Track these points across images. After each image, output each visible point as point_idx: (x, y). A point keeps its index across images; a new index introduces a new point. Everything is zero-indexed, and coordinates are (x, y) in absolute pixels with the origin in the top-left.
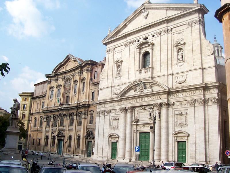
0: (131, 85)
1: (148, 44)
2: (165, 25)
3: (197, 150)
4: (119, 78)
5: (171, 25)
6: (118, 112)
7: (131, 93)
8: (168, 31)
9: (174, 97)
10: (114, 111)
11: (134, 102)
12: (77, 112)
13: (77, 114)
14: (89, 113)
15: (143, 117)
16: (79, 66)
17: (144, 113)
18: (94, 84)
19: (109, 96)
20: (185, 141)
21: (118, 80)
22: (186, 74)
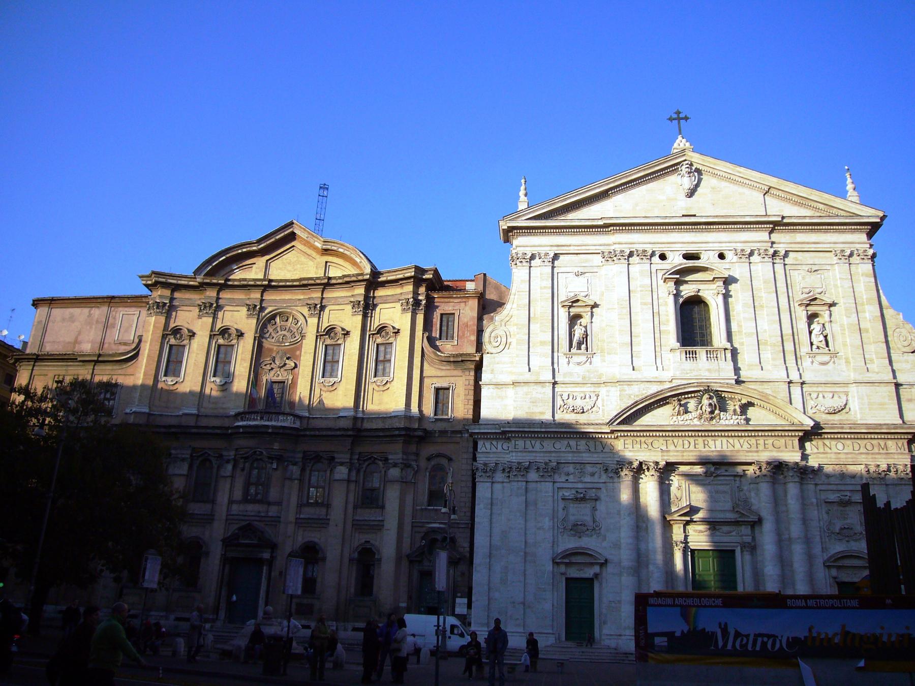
0: (667, 392)
6: (593, 475)
8: (775, 253)
10: (571, 469)
11: (672, 447)
12: (352, 454)
13: (351, 459)
14: (423, 463)
18: (452, 359)
21: (579, 364)
22: (845, 389)
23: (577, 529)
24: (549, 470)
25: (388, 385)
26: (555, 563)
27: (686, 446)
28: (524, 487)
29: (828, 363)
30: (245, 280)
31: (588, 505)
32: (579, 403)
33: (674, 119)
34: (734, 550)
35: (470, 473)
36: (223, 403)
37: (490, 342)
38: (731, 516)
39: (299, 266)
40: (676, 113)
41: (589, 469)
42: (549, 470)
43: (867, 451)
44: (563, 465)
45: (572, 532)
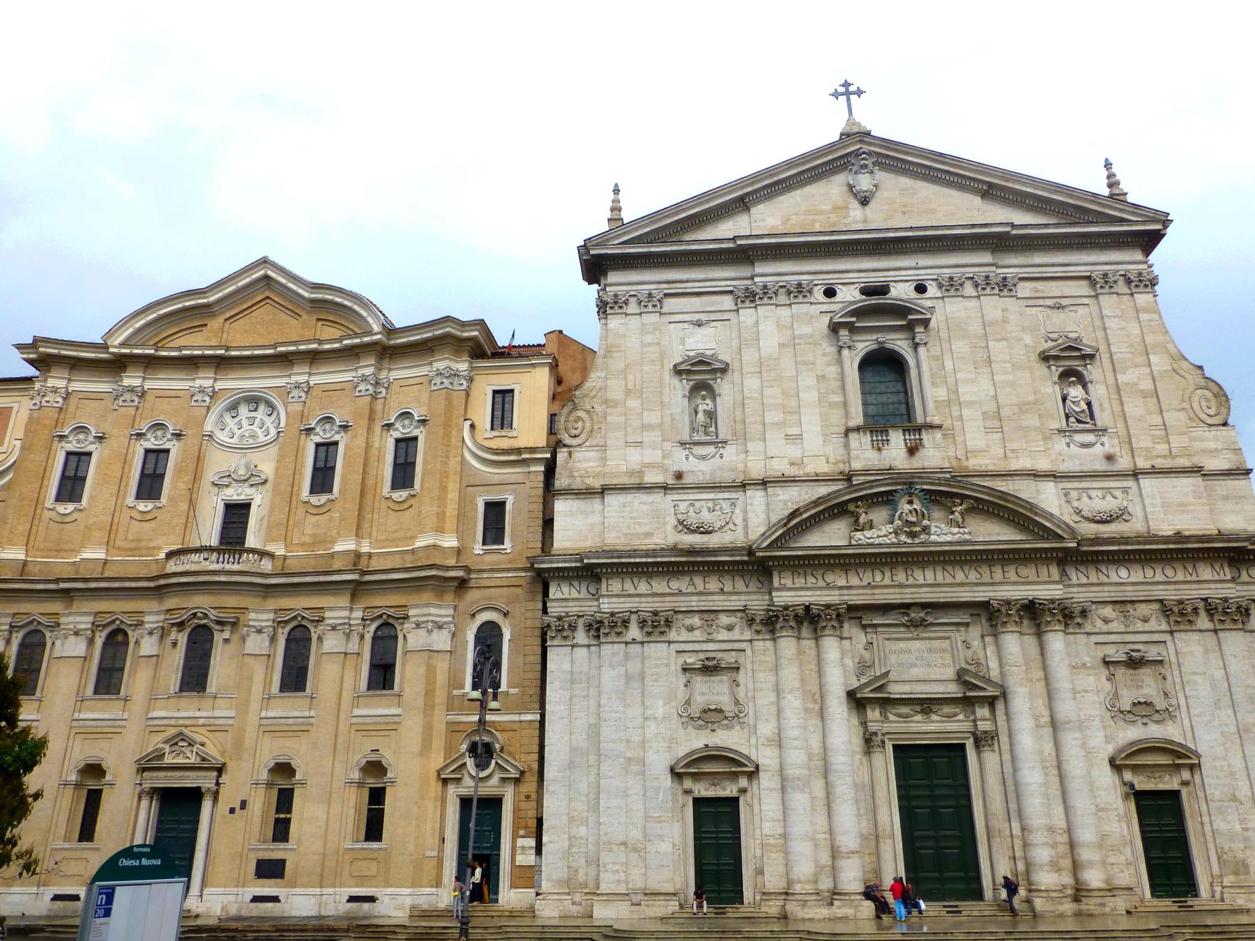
1: (910, 317)
2: (986, 258)
4: (710, 450)
5: (1013, 264)
7: (833, 536)
15: (912, 665)
16: (375, 343)
17: (917, 644)
19: (648, 535)
23: (711, 716)
24: (662, 623)
25: (412, 501)
26: (677, 775)
28: (622, 652)
29: (1093, 445)
30: (186, 348)
31: (725, 678)
32: (706, 517)
33: (842, 94)
34: (964, 744)
35: (538, 633)
36: (151, 540)
37: (566, 430)
38: (953, 690)
39: (275, 327)
40: (843, 85)
41: (724, 620)
42: (662, 623)
43: (1166, 579)
44: (680, 616)
45: (701, 723)
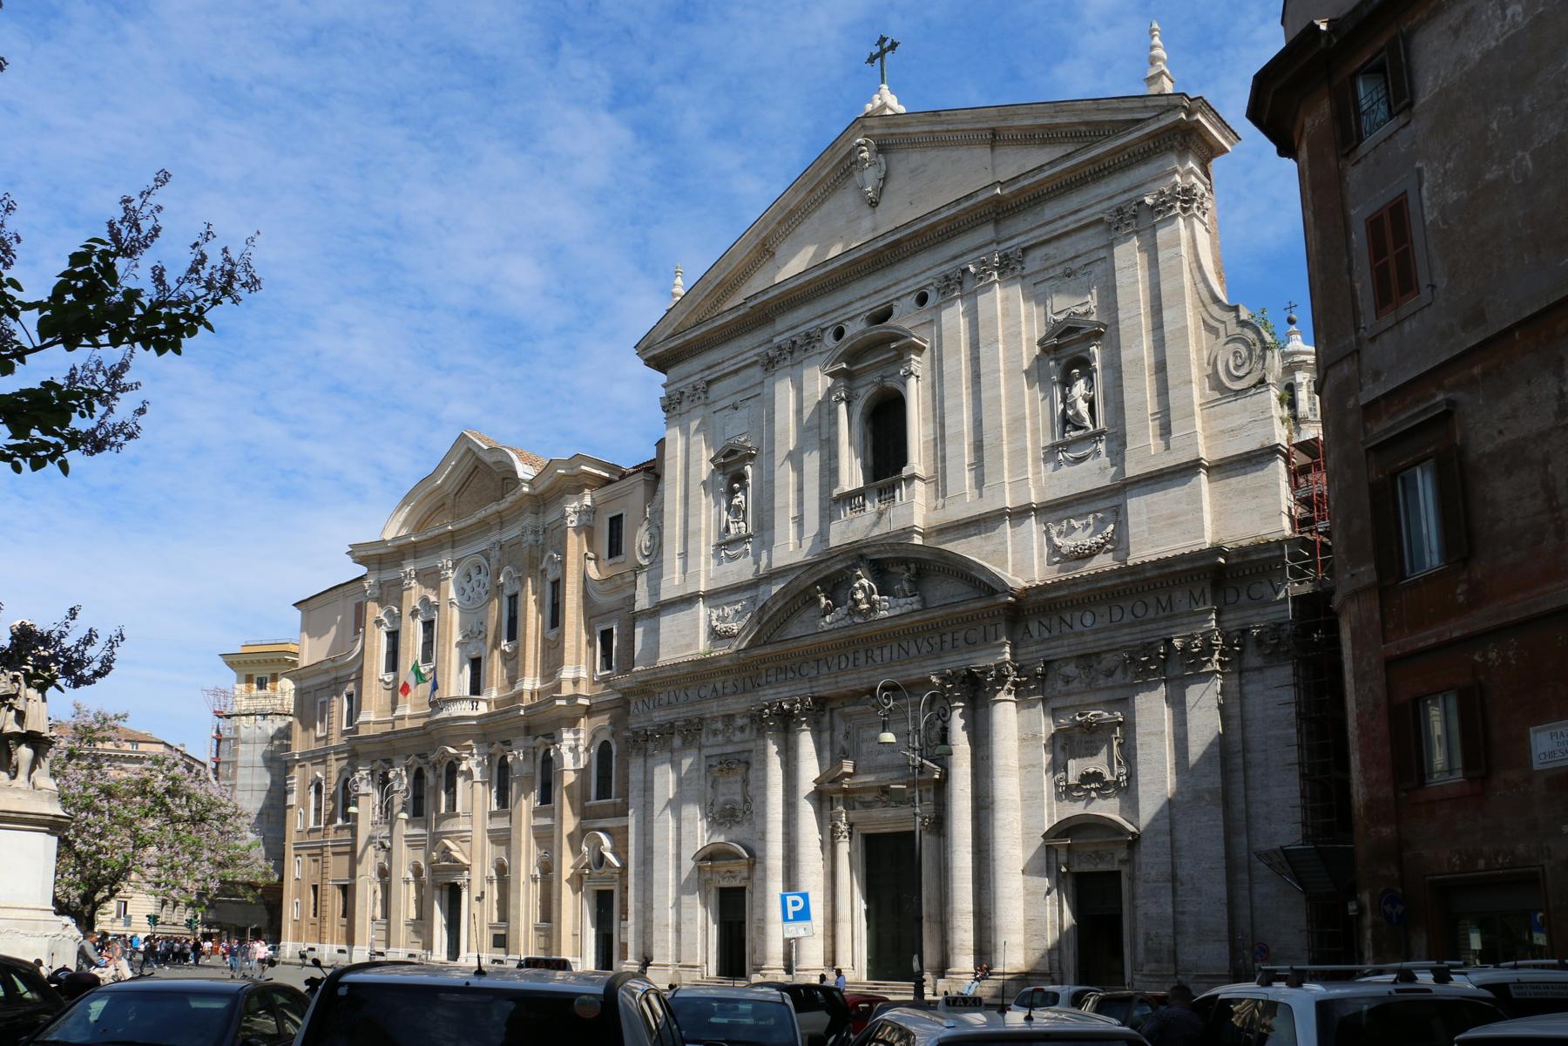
3: (1183, 913)
9: (1046, 635)
20: (1118, 873)
27: (843, 666)
